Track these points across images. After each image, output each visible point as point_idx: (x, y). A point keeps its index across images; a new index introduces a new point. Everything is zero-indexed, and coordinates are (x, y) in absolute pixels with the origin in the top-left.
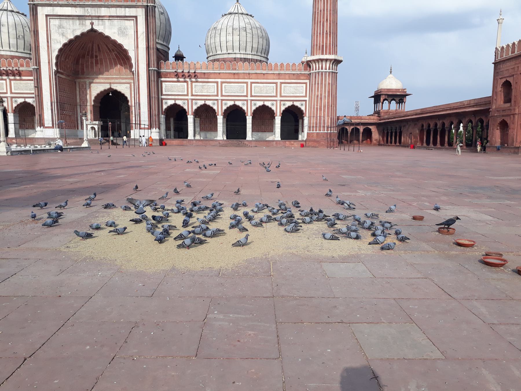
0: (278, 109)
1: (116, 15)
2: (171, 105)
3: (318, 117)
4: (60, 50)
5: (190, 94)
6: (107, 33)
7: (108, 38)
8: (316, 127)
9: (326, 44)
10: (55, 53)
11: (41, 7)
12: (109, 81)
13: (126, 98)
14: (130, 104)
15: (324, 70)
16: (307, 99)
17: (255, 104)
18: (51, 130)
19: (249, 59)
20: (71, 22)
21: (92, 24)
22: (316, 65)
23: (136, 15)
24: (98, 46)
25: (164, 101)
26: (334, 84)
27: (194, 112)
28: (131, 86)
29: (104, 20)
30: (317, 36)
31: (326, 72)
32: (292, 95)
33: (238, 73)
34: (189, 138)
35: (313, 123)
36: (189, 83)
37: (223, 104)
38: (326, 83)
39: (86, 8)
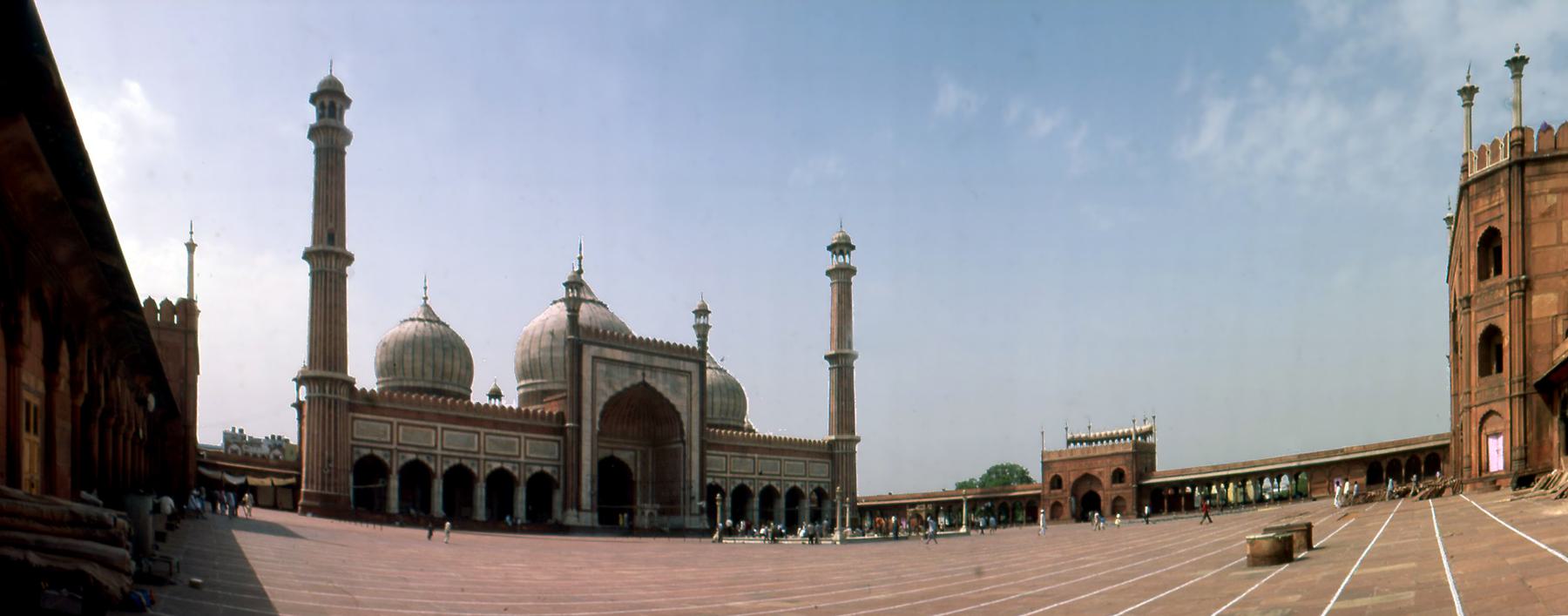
4: (607, 405)
6: (660, 388)
10: (599, 409)
13: (630, 470)
14: (634, 478)
16: (829, 480)
18: (589, 515)
21: (644, 375)
32: (818, 475)
39: (639, 355)
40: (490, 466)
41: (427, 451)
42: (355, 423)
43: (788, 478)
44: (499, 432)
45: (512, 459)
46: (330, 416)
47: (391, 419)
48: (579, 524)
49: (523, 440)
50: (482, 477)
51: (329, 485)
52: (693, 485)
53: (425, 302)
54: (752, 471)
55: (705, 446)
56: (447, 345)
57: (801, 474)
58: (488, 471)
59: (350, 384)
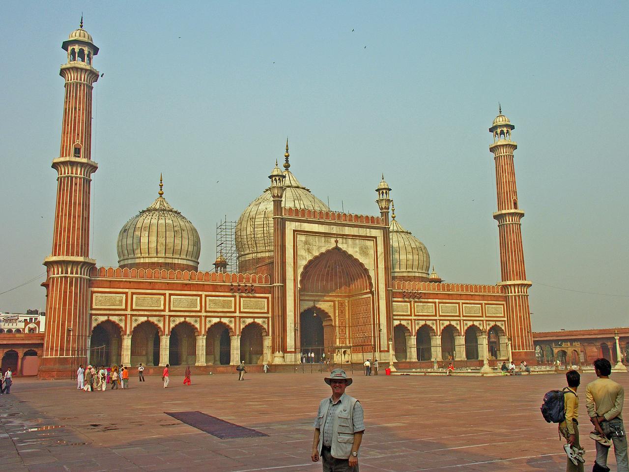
2: (397, 326)
4: (306, 267)
5: (413, 315)
6: (350, 251)
7: (351, 256)
8: (523, 346)
9: (522, 270)
10: (300, 270)
12: (314, 298)
15: (523, 294)
17: (466, 324)
20: (317, 239)
21: (337, 242)
24: (320, 261)
28: (334, 304)
30: (513, 263)
31: (524, 295)
32: (494, 315)
33: (451, 294)
35: (519, 342)
40: (210, 321)
41: (157, 313)
42: (95, 295)
43: (465, 318)
45: (228, 315)
46: (71, 292)
48: (284, 363)
51: (68, 350)
55: (391, 296)
56: (176, 229)
58: (208, 326)
59: (91, 267)
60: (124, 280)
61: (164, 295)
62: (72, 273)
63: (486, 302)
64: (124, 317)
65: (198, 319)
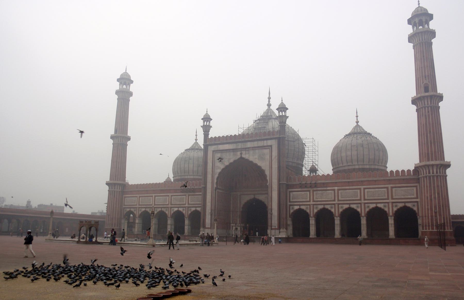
0: (391, 210)
1: (257, 146)
2: (297, 210)
3: (430, 217)
4: (220, 174)
5: (312, 201)
7: (252, 162)
9: (431, 151)
10: (216, 176)
11: (210, 146)
16: (418, 200)
17: (368, 207)
19: (367, 169)
20: (228, 154)
21: (241, 154)
22: (423, 170)
23: (271, 145)
25: (291, 207)
26: (444, 186)
27: (315, 215)
29: (249, 151)
31: (433, 176)
32: (403, 197)
34: (311, 237)
35: (426, 223)
36: (311, 192)
37: (340, 208)
38: (435, 185)
39: (238, 144)
40: (173, 210)
42: (126, 198)
44: (177, 194)
47: (137, 195)
49: (187, 196)
50: (169, 216)
52: (273, 211)
53: (196, 141)
54: (333, 199)
57: (384, 198)
58: (172, 212)
60: (136, 190)
61: (152, 196)
62: (111, 189)
63: (394, 185)
64: (136, 209)
65: (167, 209)
